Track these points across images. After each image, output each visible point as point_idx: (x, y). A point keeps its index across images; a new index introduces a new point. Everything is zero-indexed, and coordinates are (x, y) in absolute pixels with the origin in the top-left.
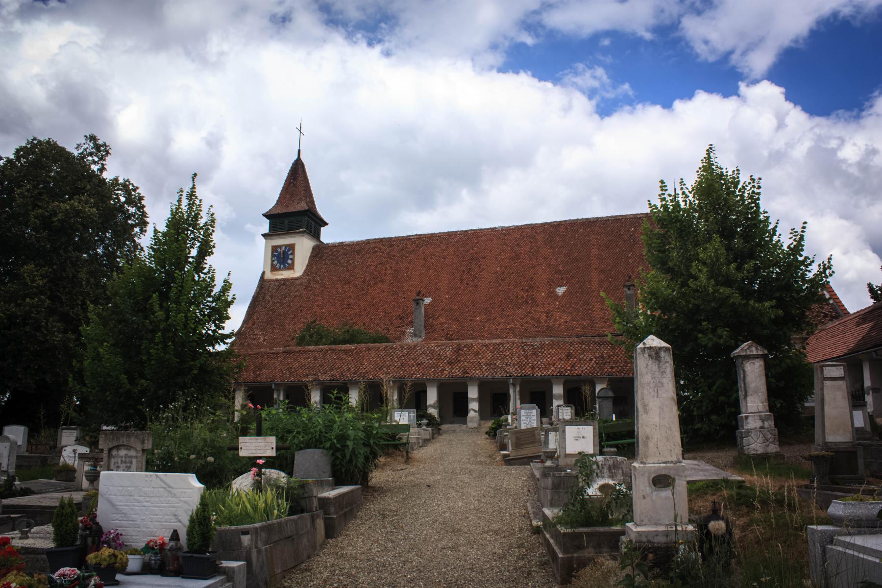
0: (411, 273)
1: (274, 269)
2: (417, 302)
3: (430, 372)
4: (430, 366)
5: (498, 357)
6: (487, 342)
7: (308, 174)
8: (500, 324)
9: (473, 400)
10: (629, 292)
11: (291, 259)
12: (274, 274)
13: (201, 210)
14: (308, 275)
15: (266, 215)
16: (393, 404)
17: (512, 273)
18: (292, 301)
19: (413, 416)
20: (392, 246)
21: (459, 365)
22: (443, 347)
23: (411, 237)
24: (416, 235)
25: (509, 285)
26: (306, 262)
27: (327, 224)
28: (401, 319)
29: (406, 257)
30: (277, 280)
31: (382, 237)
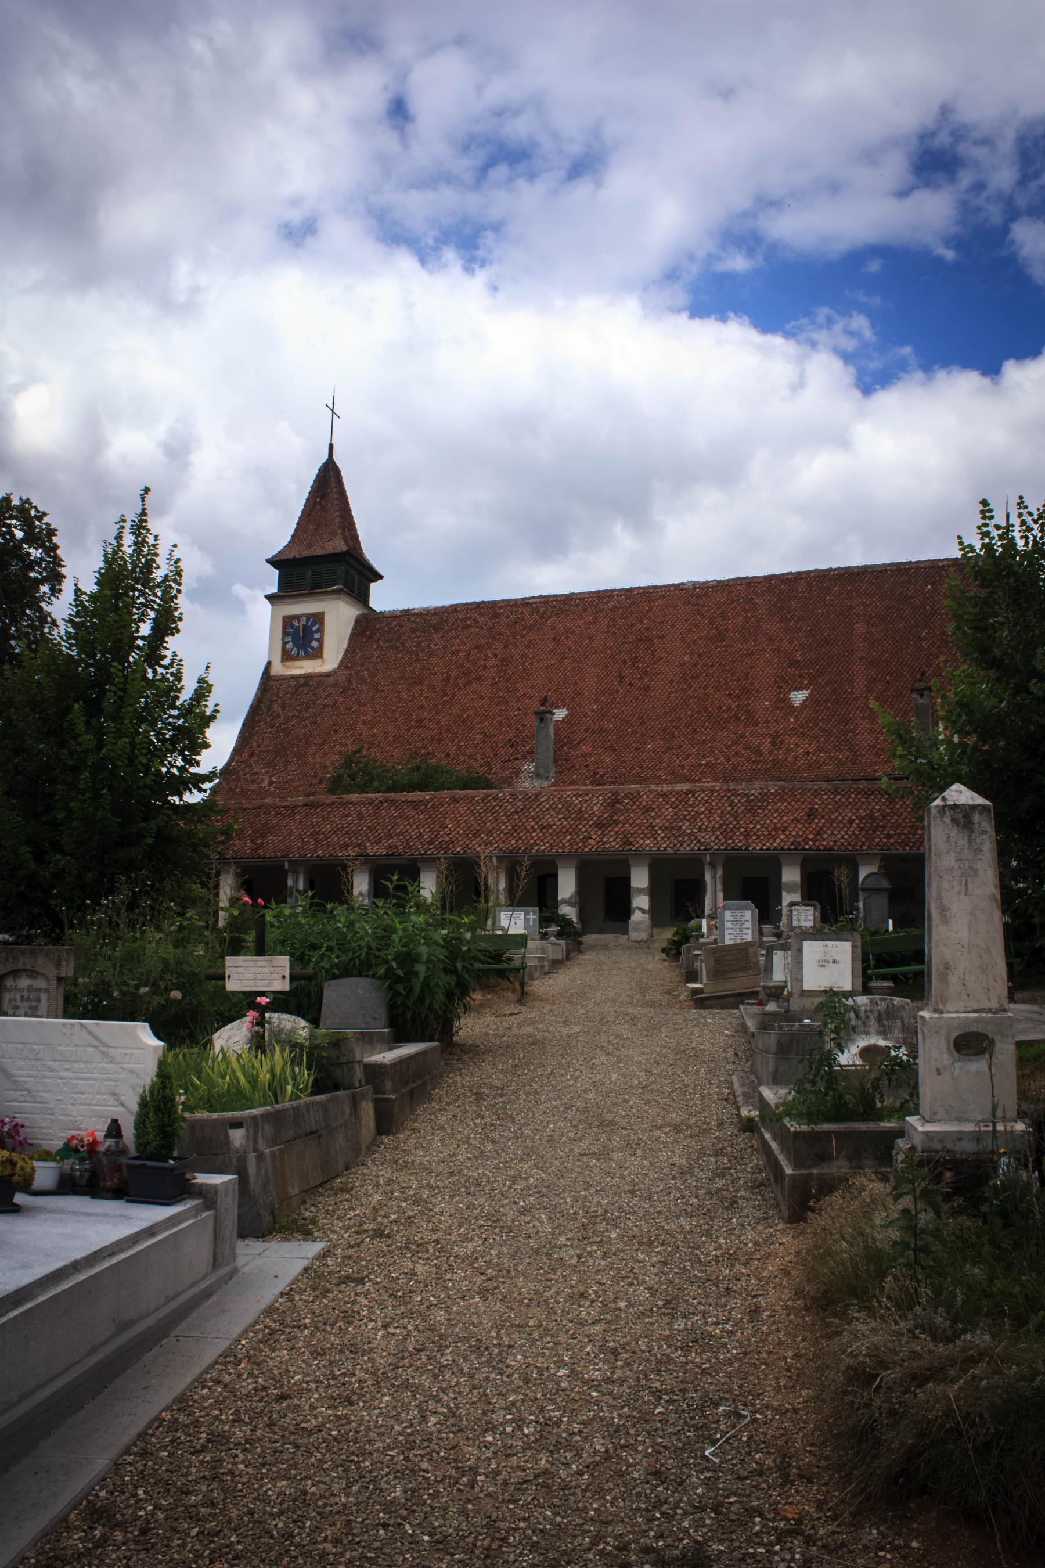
0: (531, 664)
2: (542, 716)
3: (564, 841)
4: (564, 830)
5: (685, 816)
6: (666, 788)
7: (346, 487)
8: (688, 756)
9: (640, 891)
10: (921, 701)
11: (318, 640)
12: (288, 667)
13: (157, 555)
14: (347, 668)
15: (273, 562)
16: (497, 898)
17: (712, 666)
18: (320, 714)
19: (534, 920)
20: (496, 616)
21: (616, 829)
22: (587, 798)
23: (531, 601)
24: (541, 597)
25: (705, 688)
26: (345, 645)
27: (381, 577)
28: (512, 746)
29: (523, 636)
30: (293, 677)
31: (478, 600)
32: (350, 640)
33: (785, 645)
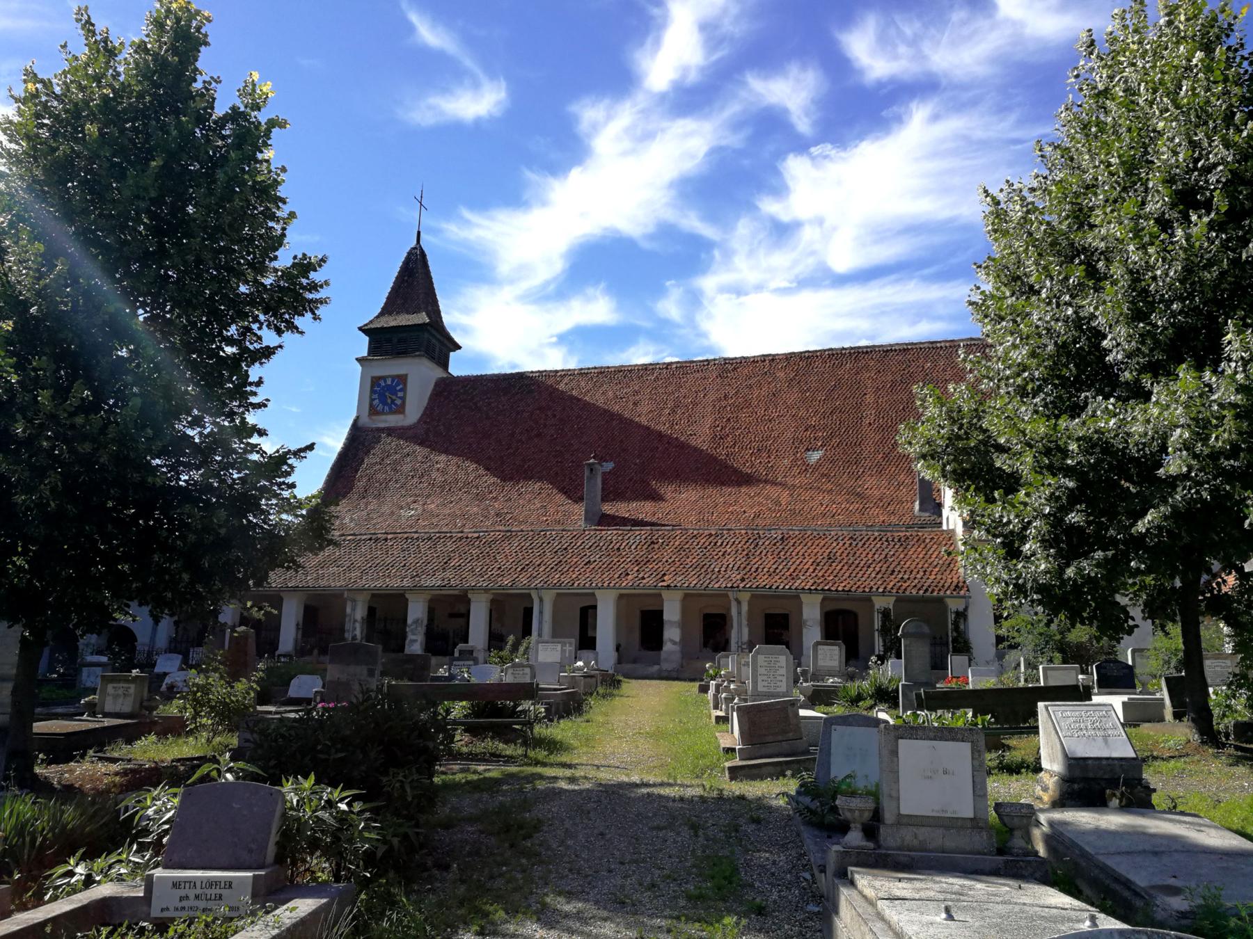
1: (373, 411)
14: (425, 422)
19: (570, 651)
26: (425, 404)
32: (431, 399)
33: (802, 413)
